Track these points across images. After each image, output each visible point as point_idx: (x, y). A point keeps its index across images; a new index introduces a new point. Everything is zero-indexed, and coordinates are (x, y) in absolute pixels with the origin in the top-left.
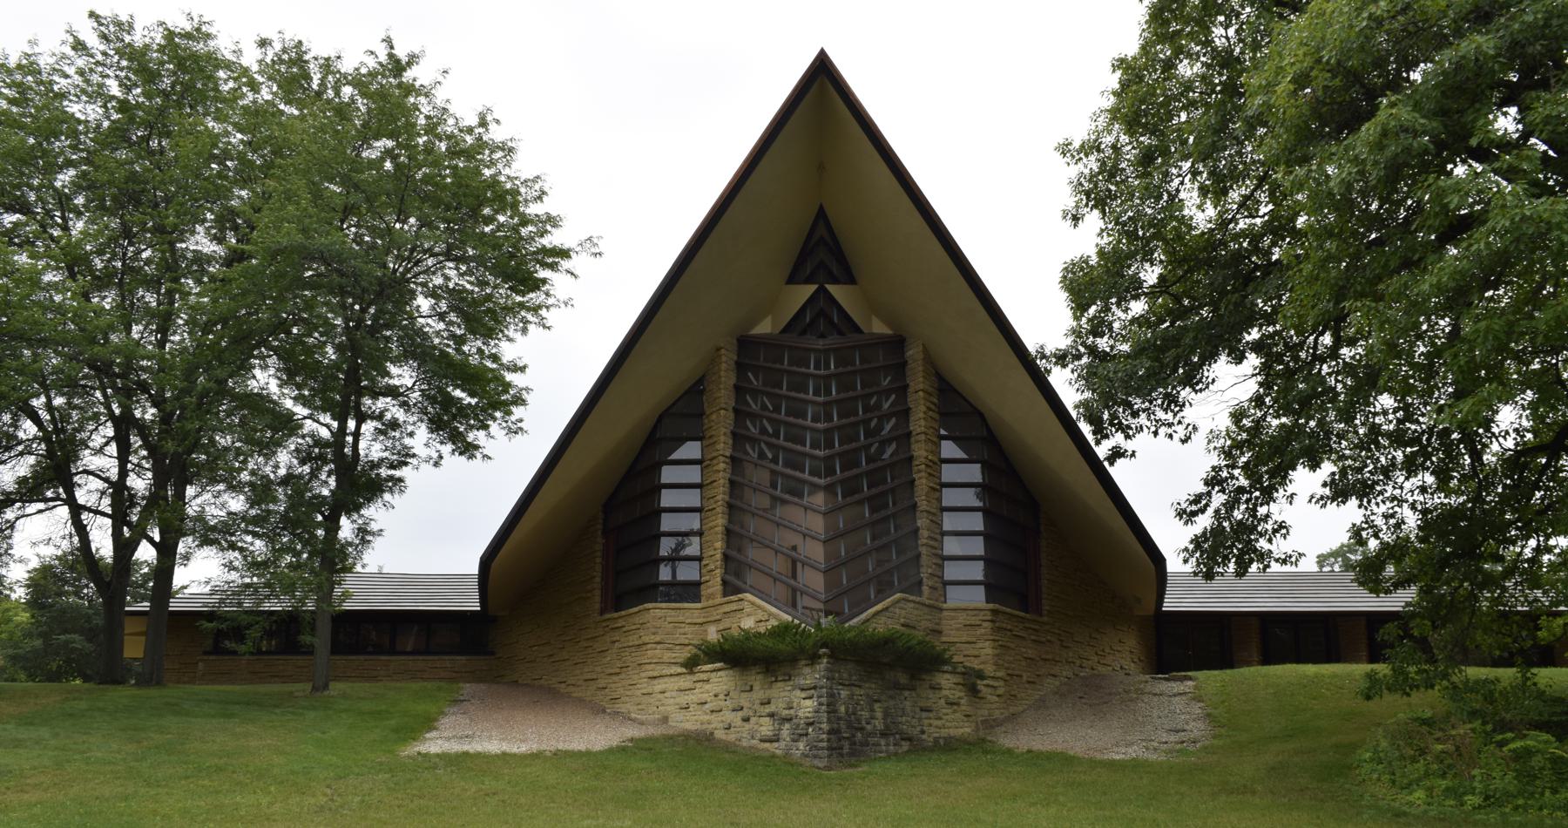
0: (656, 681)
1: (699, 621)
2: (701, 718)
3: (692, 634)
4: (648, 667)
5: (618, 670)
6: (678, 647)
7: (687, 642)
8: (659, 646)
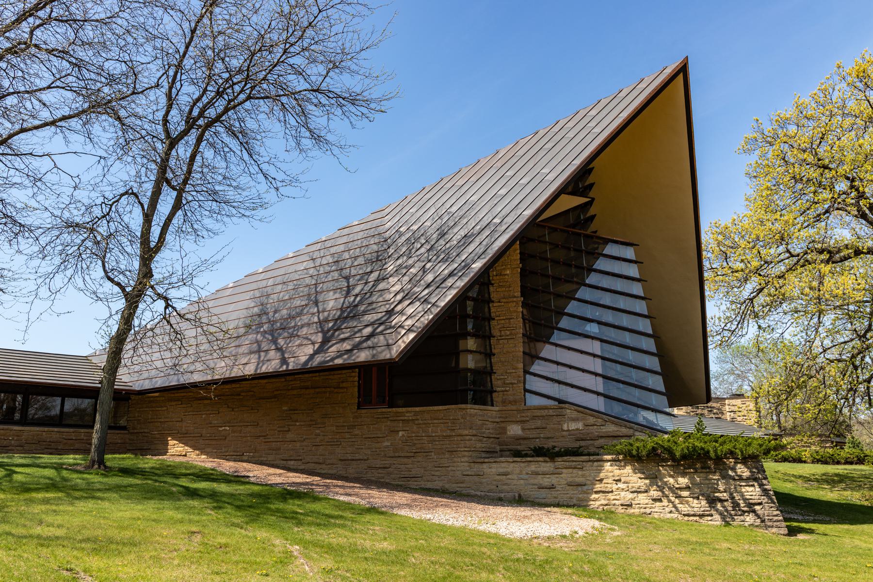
0: (485, 466)
1: (497, 420)
2: (580, 496)
3: (492, 429)
4: (466, 453)
5: (412, 454)
6: (485, 439)
7: (491, 436)
8: (473, 438)
